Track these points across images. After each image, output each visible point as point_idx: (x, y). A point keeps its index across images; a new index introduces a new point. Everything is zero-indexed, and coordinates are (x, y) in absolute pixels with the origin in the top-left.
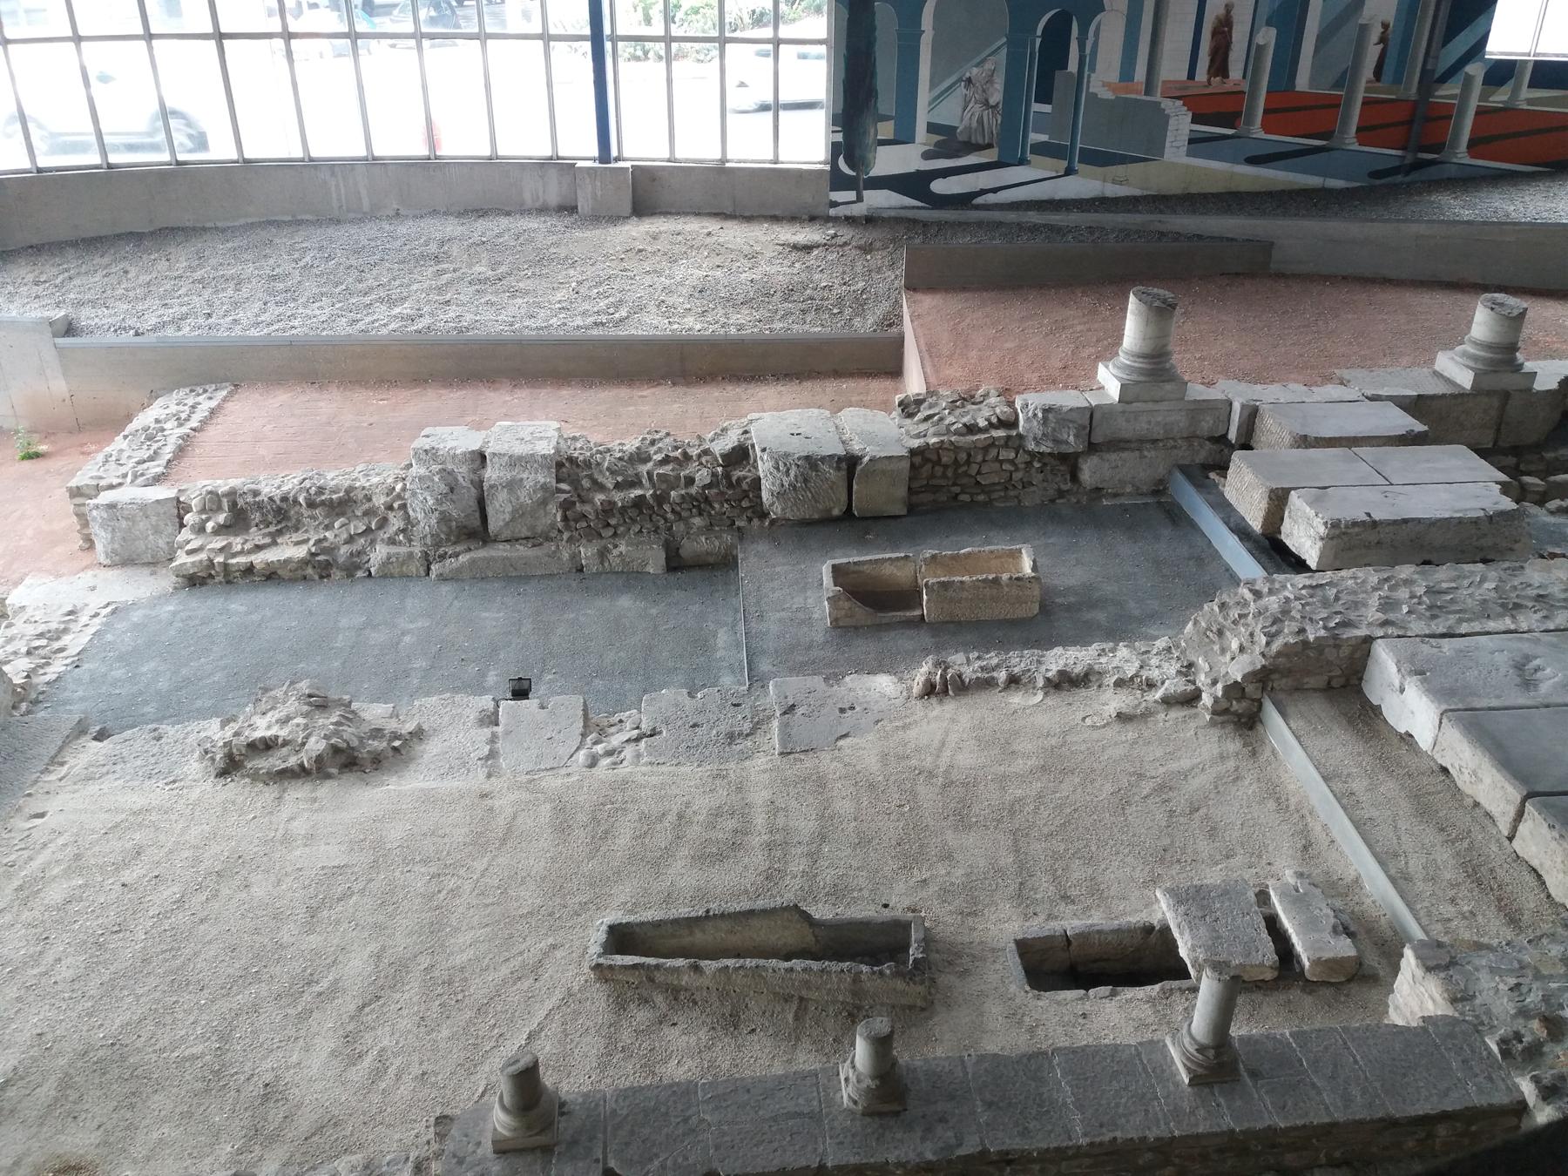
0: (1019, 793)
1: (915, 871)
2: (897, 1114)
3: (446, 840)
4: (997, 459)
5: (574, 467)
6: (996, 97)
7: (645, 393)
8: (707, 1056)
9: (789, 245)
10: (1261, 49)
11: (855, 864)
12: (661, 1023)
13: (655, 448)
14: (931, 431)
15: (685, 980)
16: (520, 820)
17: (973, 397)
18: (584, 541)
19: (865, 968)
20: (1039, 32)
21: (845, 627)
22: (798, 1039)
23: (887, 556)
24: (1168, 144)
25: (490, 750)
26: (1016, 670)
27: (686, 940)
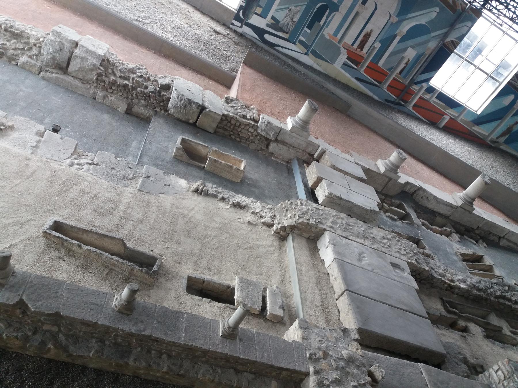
0: (209, 233)
1: (166, 244)
2: (128, 315)
3: (7, 168)
4: (248, 130)
5: (108, 63)
6: (296, 19)
7: (143, 51)
8: (72, 275)
9: (213, 29)
10: (374, 48)
11: (148, 234)
12: (60, 258)
13: (139, 71)
14: (232, 111)
15: (74, 248)
16: (37, 173)
17: (249, 107)
18: (100, 90)
19: (137, 267)
20: (317, 7)
21: (178, 159)
22: (105, 280)
23: (201, 143)
24: (337, 61)
25: (36, 145)
26: (225, 196)
27: (80, 236)
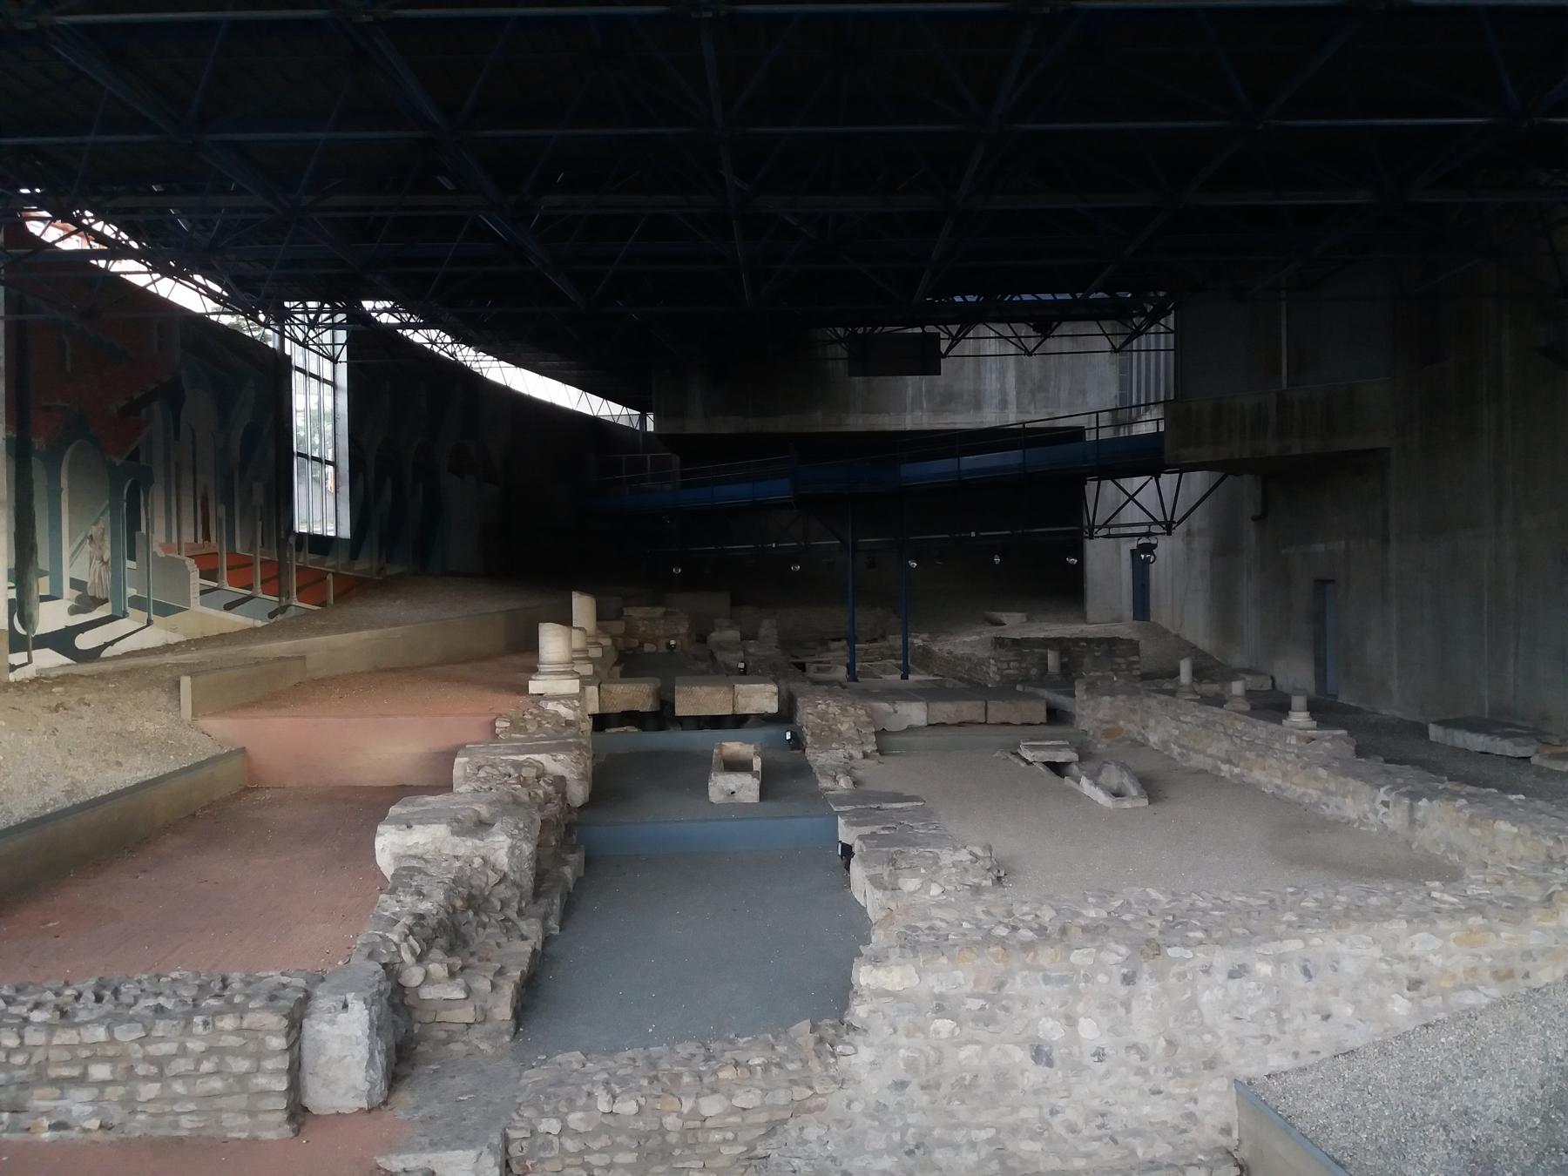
6: (107, 556)
20: (125, 498)
24: (192, 596)
